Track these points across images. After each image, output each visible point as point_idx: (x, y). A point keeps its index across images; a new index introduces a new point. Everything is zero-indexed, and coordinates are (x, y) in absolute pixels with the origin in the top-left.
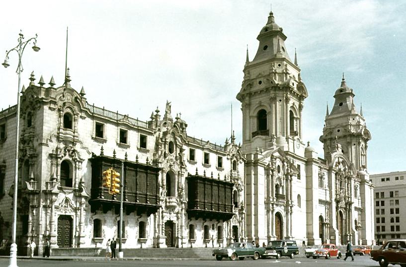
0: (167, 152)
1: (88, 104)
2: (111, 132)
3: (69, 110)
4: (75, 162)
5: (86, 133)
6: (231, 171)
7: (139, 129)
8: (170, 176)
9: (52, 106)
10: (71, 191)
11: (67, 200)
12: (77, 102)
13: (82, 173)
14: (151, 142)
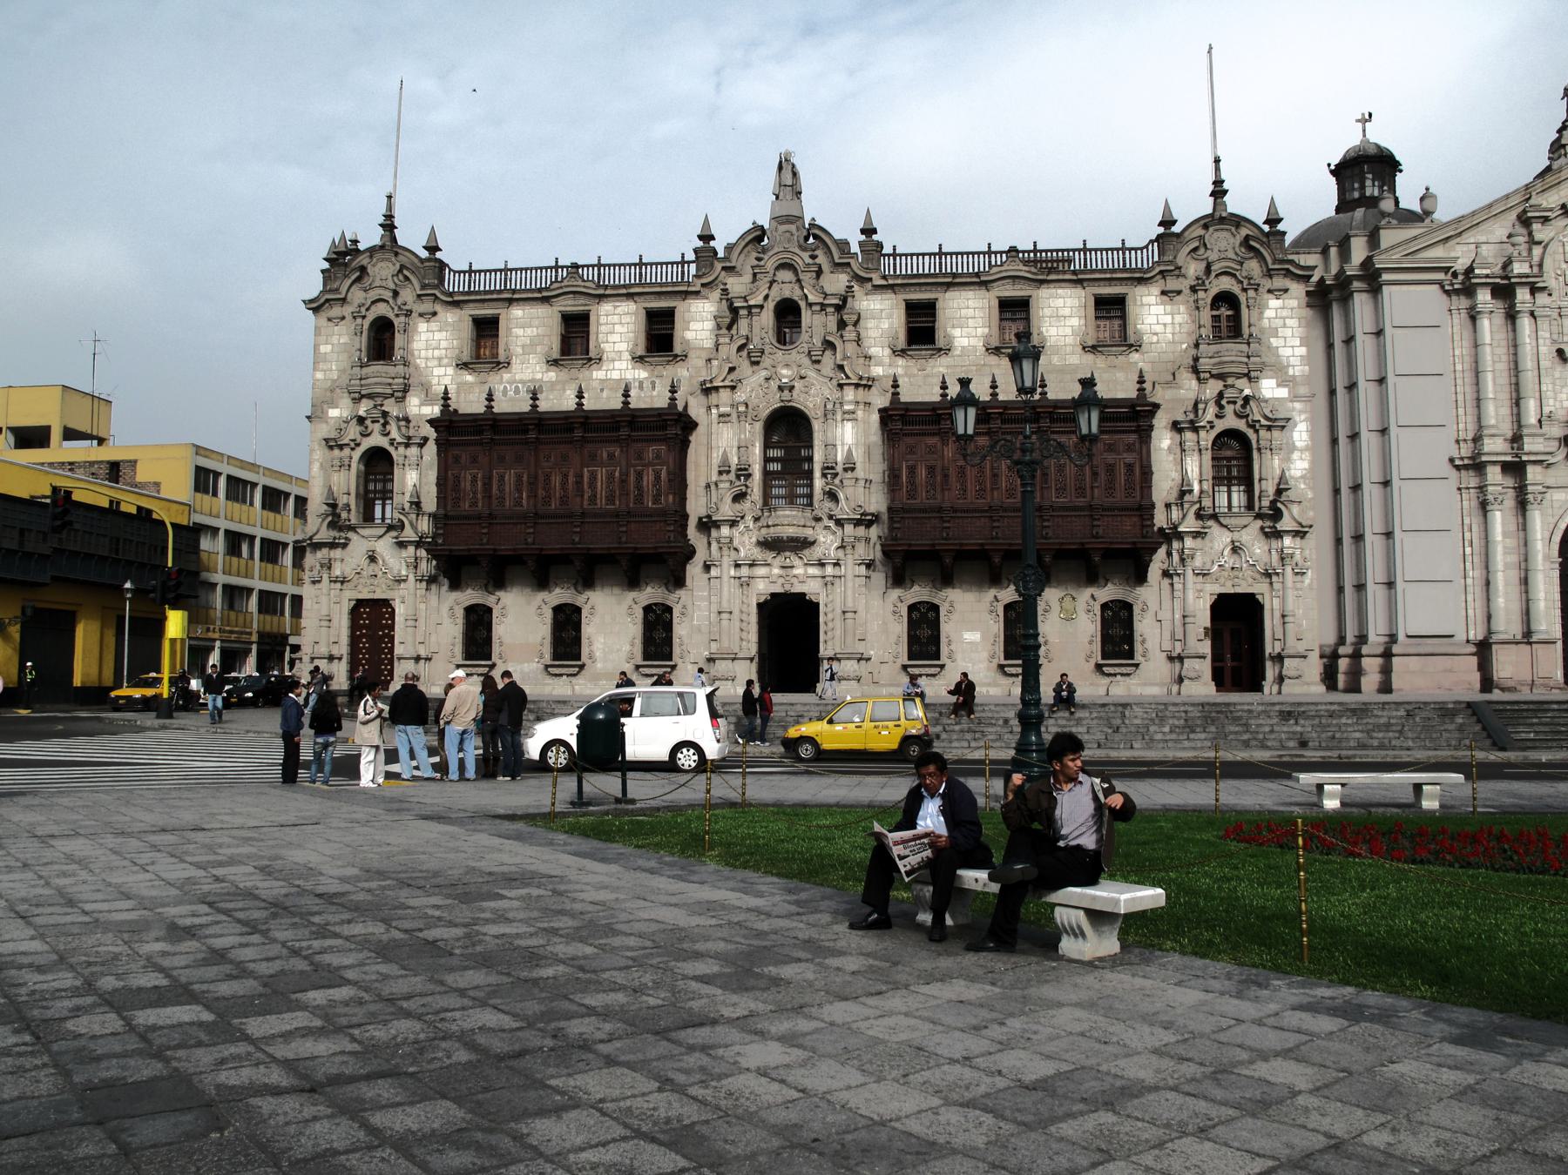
2: (529, 331)
3: (381, 310)
8: (789, 428)
9: (336, 311)
12: (407, 278)
13: (416, 477)
14: (698, 323)
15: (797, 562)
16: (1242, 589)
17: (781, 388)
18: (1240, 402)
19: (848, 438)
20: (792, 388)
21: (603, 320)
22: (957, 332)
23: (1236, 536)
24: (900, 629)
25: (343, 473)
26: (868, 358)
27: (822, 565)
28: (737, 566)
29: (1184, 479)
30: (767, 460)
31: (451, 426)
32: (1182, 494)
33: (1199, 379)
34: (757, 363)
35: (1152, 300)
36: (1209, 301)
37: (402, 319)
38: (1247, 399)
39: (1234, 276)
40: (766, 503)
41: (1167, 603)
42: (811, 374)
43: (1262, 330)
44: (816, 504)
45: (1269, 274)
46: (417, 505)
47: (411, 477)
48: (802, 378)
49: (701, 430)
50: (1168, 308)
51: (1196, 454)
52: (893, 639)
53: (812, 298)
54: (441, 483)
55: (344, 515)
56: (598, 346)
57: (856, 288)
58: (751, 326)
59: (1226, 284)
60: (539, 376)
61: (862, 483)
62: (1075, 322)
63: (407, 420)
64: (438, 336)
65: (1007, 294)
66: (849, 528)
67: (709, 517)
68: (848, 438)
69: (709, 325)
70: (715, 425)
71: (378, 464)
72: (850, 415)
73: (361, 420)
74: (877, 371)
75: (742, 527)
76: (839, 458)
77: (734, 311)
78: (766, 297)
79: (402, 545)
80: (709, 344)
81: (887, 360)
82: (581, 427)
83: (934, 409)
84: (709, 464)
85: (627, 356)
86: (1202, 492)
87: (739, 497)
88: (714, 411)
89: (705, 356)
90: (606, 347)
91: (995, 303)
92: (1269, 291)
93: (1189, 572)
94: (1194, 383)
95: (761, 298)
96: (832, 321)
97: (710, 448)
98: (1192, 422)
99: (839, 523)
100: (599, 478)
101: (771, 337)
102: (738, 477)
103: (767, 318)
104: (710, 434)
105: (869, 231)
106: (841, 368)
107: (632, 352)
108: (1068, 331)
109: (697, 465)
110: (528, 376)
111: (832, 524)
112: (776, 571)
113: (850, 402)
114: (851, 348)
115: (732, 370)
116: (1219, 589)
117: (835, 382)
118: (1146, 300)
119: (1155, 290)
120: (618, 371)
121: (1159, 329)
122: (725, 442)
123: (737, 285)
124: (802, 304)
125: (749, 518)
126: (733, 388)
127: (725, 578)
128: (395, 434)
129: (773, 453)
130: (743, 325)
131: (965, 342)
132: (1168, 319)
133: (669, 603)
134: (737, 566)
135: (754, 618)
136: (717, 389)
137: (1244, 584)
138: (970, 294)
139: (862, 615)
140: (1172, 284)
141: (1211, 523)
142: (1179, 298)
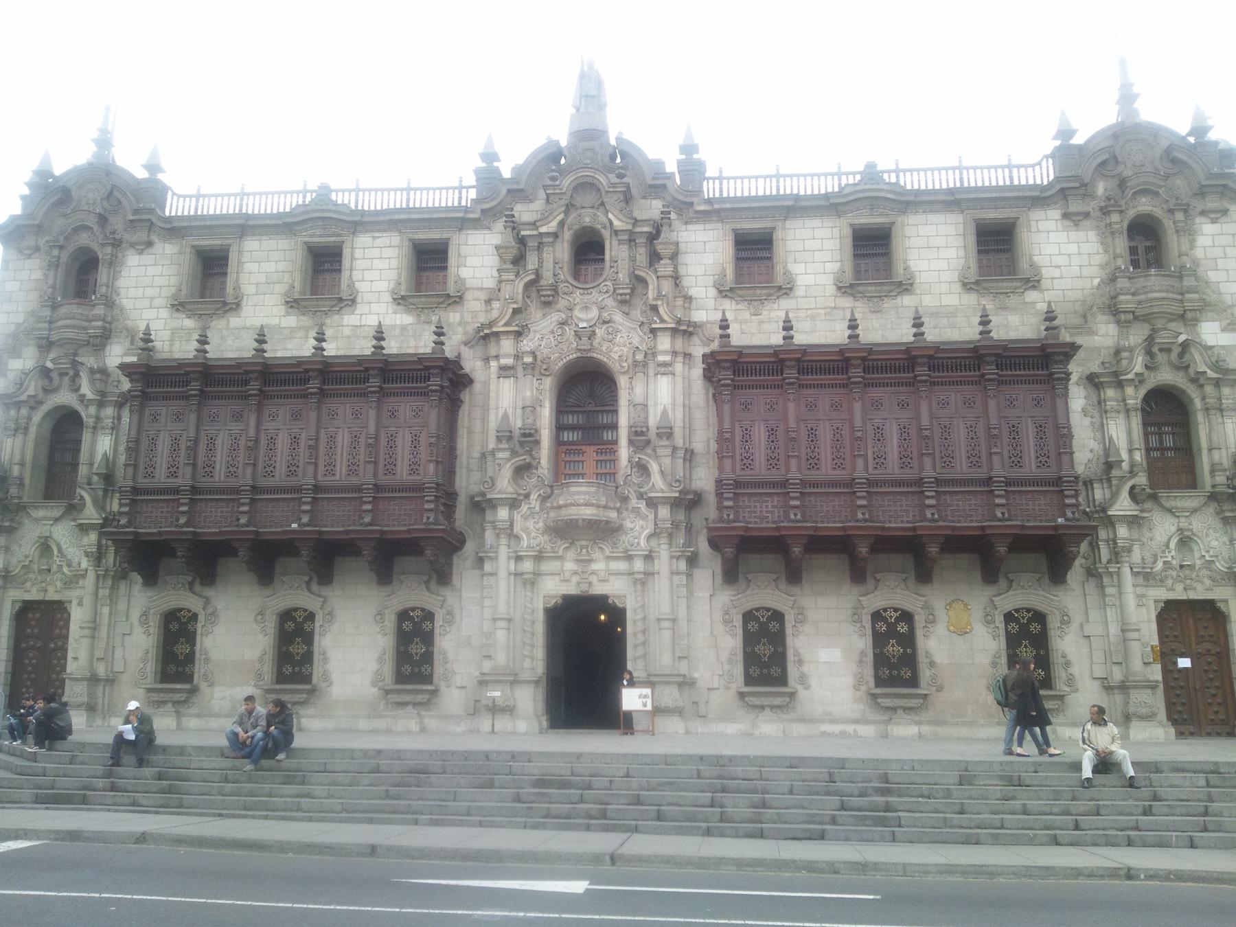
0: (548, 278)
1: (174, 194)
3: (84, 239)
4: (87, 406)
5: (152, 299)
6: (1113, 279)
7: (718, 211)
8: (586, 389)
10: (57, 513)
11: (45, 547)
15: (597, 554)
16: (1199, 594)
17: (578, 335)
18: (1176, 350)
19: (663, 396)
20: (592, 335)
21: (358, 253)
22: (796, 269)
23: (1184, 523)
24: (732, 642)
25: (20, 438)
26: (691, 298)
27: (629, 558)
28: (519, 559)
29: (1109, 449)
30: (560, 428)
31: (155, 381)
32: (1109, 466)
33: (1118, 322)
34: (547, 304)
35: (1051, 225)
36: (1126, 224)
37: (109, 250)
38: (1185, 346)
39: (1156, 194)
40: (557, 479)
41: (1094, 615)
42: (618, 317)
43: (1196, 263)
44: (621, 480)
45: (1202, 192)
46: (108, 478)
47: (104, 444)
48: (605, 322)
49: (477, 387)
50: (1073, 235)
51: (1122, 416)
52: (725, 656)
53: (616, 223)
54: (134, 448)
55: (13, 491)
56: (351, 285)
57: (673, 216)
58: (541, 262)
59: (1145, 205)
60: (274, 321)
61: (681, 453)
62: (952, 253)
63: (104, 371)
64: (152, 271)
65: (862, 221)
66: (664, 512)
67: (483, 494)
68: (663, 396)
69: (493, 261)
70: (494, 381)
71: (65, 429)
72: (665, 368)
73: (45, 372)
74: (699, 316)
75: (524, 508)
76: (653, 422)
77: (522, 241)
78: (562, 223)
79: (84, 529)
80: (490, 283)
81: (711, 303)
82: (323, 380)
83: (776, 353)
84: (485, 431)
85: (387, 297)
86: (1133, 465)
87: (522, 470)
88: (493, 364)
89: (483, 296)
90: (360, 286)
91: (848, 232)
92: (1203, 213)
93: (1126, 571)
94: (1112, 329)
95: (554, 224)
96: (642, 254)
97: (485, 408)
98: (1116, 374)
99: (652, 503)
100: (342, 444)
101: (565, 274)
102: (522, 444)
103: (563, 251)
104: (486, 394)
105: (689, 149)
106: (654, 309)
107: (393, 292)
108: (943, 265)
109: (470, 432)
110: (264, 317)
111: (642, 505)
112: (570, 566)
113: (665, 352)
114: (667, 286)
115: (516, 312)
116: (1163, 594)
117: (646, 328)
118: (1043, 225)
119: (1055, 214)
120: (376, 314)
121: (1061, 260)
122: (509, 399)
123: (525, 212)
124: (606, 234)
125: (533, 497)
126: (518, 334)
127: (503, 574)
128: (86, 390)
129: (570, 419)
130: (532, 262)
131: (810, 280)
132: (1073, 248)
133: (428, 607)
134: (519, 559)
135: (540, 628)
136: (497, 334)
137: (1199, 587)
138: (817, 222)
139: (681, 620)
140: (1075, 206)
141: (1148, 505)
142: (1087, 223)
